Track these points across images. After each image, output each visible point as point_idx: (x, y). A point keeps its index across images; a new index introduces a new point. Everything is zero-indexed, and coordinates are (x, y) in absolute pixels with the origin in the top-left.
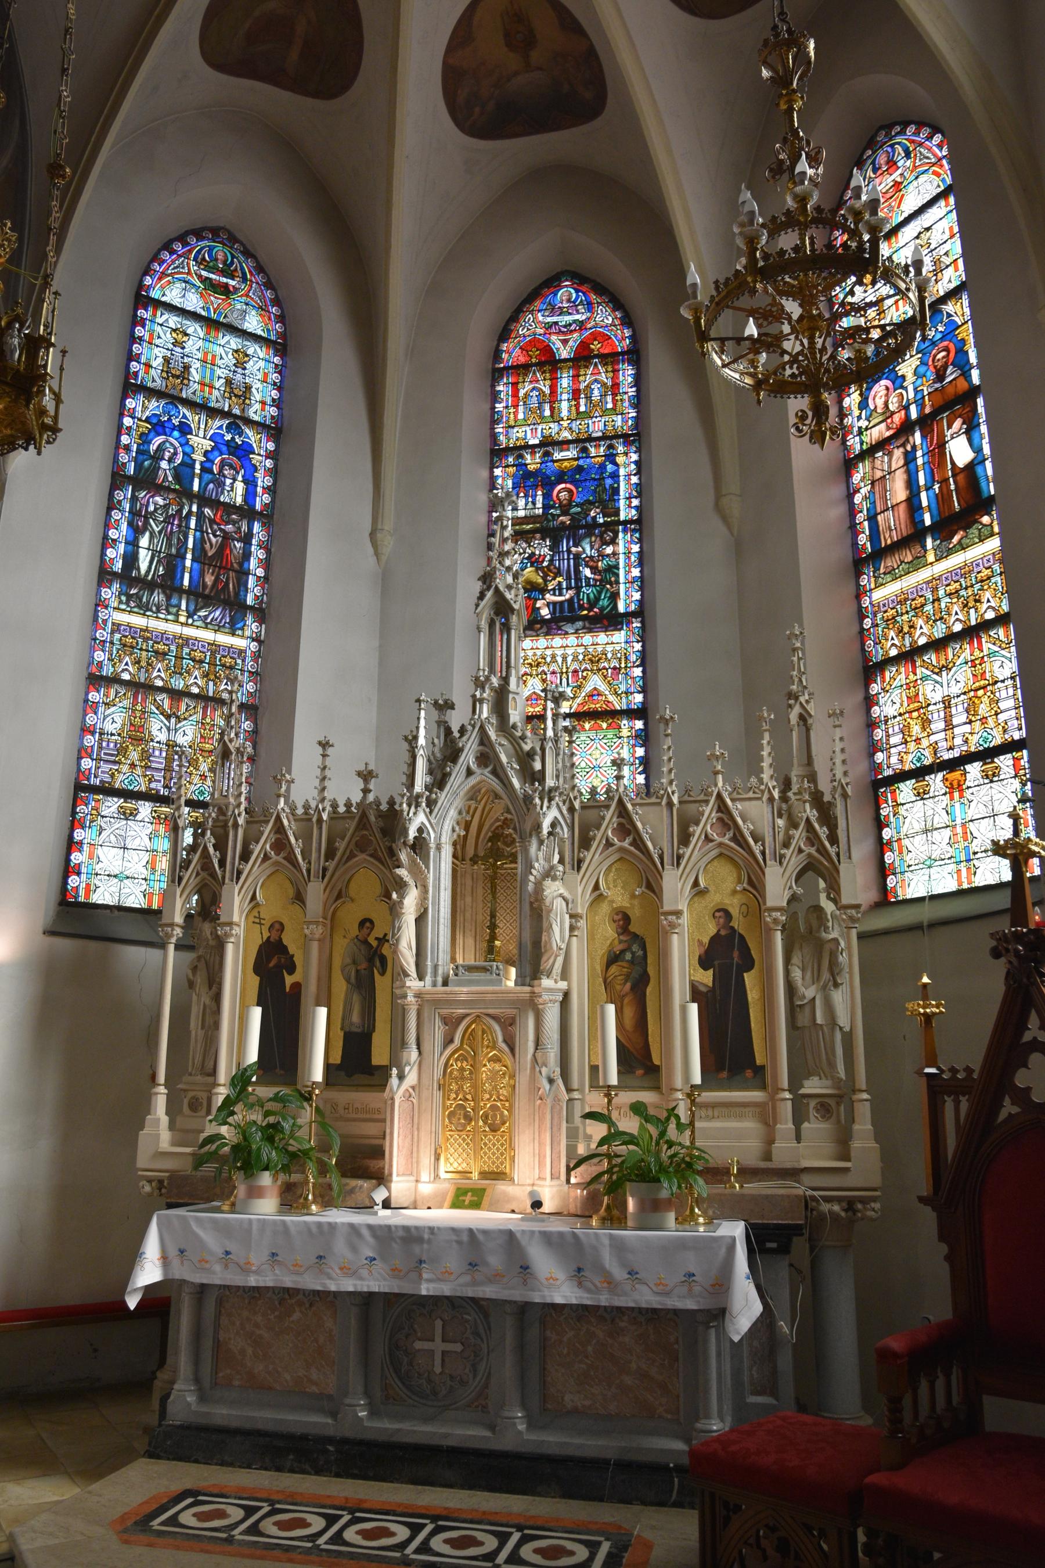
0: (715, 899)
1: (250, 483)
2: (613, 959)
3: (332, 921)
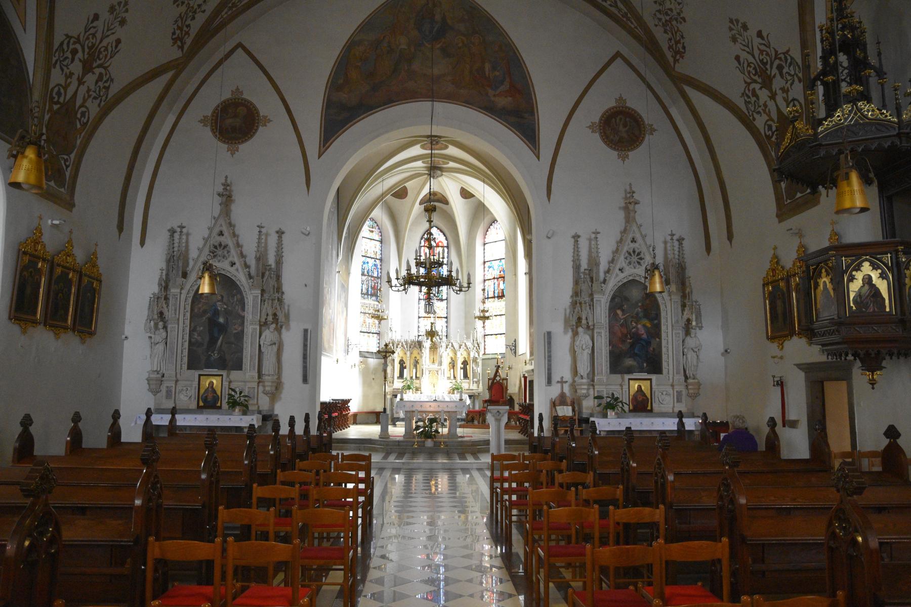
0: (464, 356)
1: (378, 272)
2: (450, 363)
3: (410, 357)
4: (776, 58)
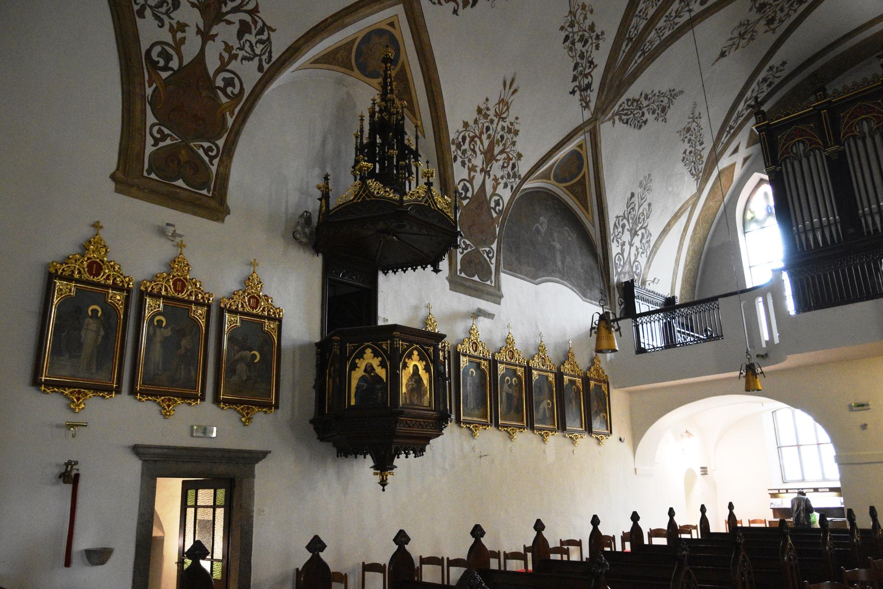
4: (250, 12)
